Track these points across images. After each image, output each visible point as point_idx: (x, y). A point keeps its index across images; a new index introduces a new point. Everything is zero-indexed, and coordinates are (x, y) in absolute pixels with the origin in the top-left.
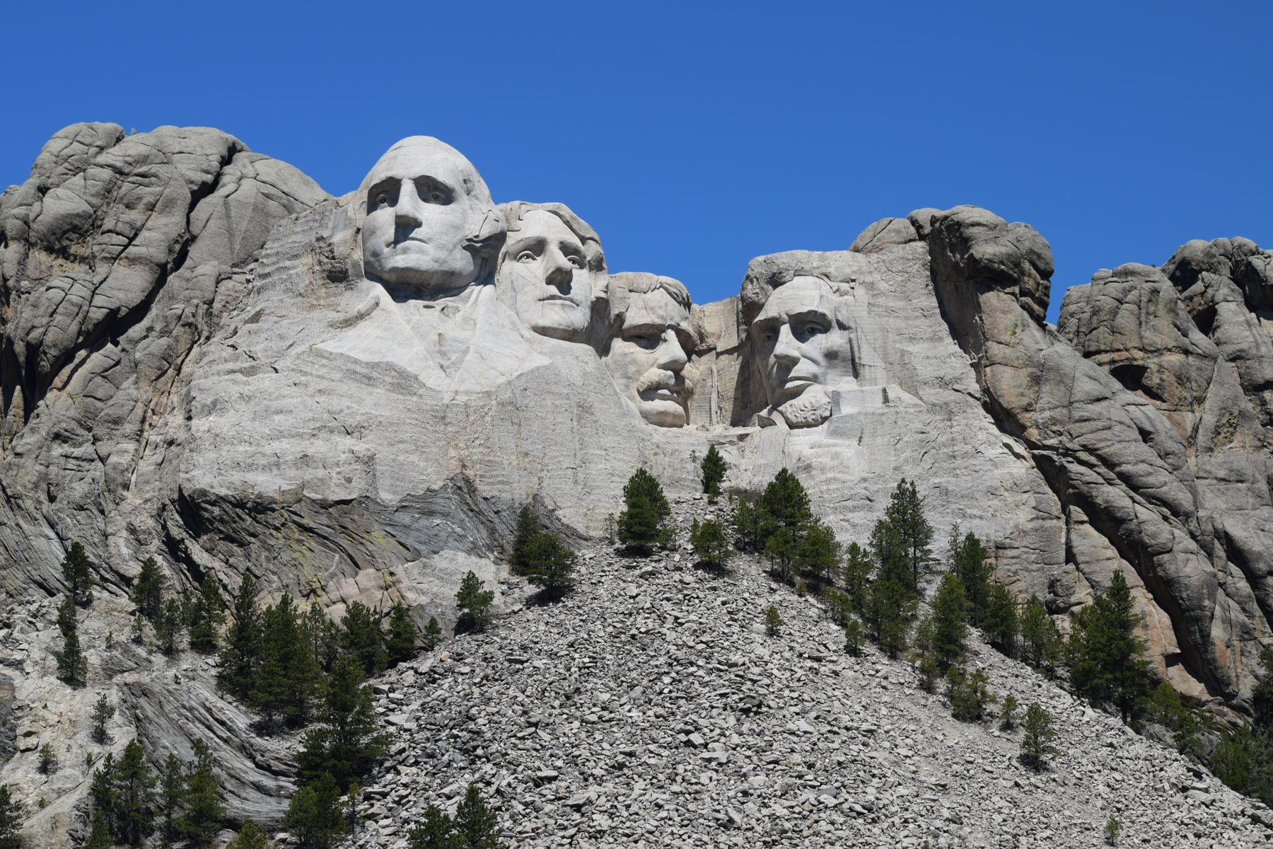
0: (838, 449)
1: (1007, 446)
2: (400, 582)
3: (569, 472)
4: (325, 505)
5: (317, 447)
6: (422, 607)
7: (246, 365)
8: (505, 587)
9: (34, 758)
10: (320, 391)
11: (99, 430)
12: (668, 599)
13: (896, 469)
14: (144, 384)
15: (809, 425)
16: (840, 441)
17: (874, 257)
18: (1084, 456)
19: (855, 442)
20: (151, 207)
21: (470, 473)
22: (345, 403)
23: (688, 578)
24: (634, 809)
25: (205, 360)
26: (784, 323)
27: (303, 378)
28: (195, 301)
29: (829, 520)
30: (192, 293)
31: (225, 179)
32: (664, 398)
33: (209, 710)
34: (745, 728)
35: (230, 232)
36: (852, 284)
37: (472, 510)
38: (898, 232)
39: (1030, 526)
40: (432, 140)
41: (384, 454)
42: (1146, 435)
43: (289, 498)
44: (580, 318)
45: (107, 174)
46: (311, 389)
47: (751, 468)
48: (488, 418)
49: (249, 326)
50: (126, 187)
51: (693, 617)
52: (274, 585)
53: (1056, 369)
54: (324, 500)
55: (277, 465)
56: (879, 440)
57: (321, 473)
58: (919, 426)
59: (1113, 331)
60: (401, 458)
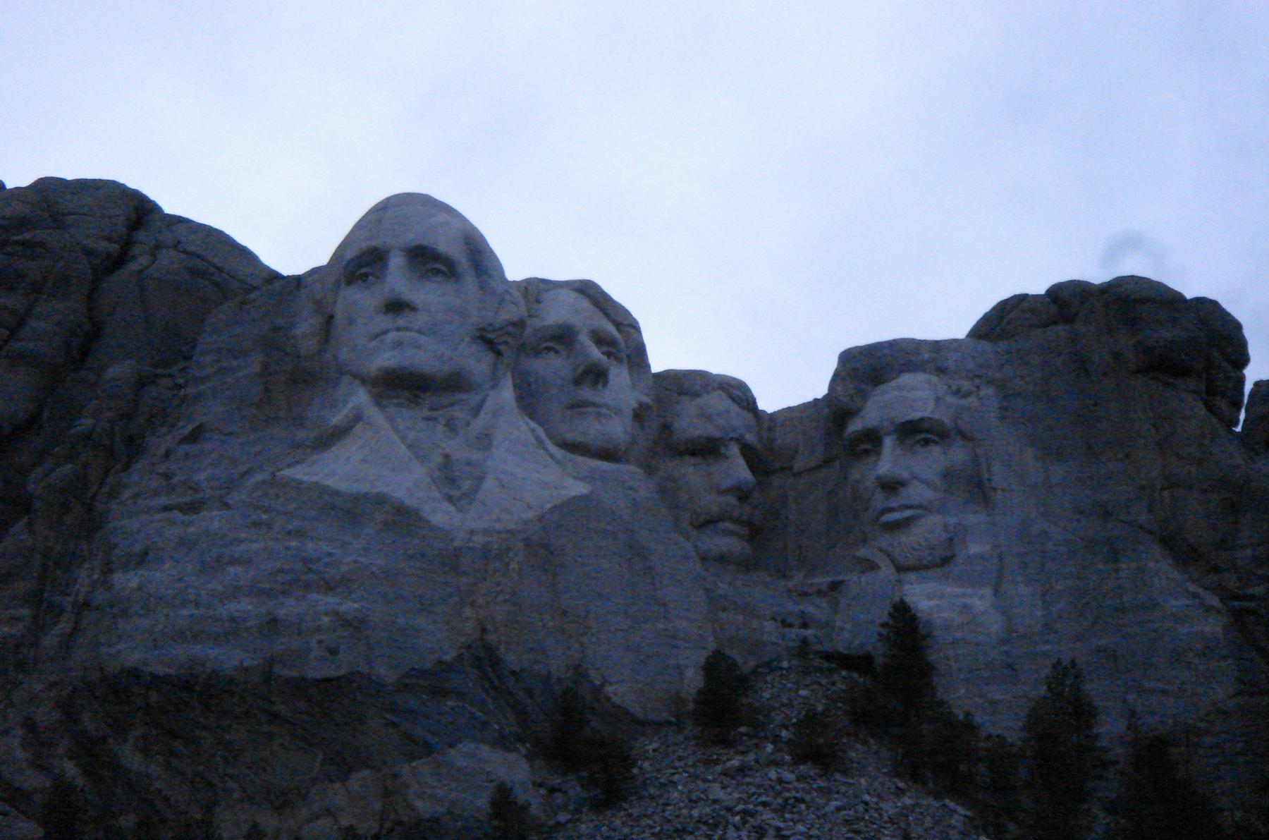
0: (968, 601)
1: (1195, 595)
2: (407, 786)
3: (619, 634)
4: (300, 686)
5: (289, 608)
6: (435, 820)
7: (188, 499)
8: (543, 791)
10: (289, 533)
12: (765, 804)
13: (1045, 625)
15: (926, 568)
16: (969, 590)
17: (1003, 345)
19: (988, 591)
20: (37, 288)
21: (491, 638)
22: (325, 547)
23: (788, 776)
25: (126, 495)
26: (888, 434)
27: (265, 517)
28: (109, 414)
29: (959, 696)
31: (137, 250)
36: (977, 381)
37: (495, 688)
44: (618, 429)
47: (857, 626)
48: (514, 565)
49: (185, 447)
51: (800, 827)
52: (235, 796)
54: (303, 679)
60: (401, 621)
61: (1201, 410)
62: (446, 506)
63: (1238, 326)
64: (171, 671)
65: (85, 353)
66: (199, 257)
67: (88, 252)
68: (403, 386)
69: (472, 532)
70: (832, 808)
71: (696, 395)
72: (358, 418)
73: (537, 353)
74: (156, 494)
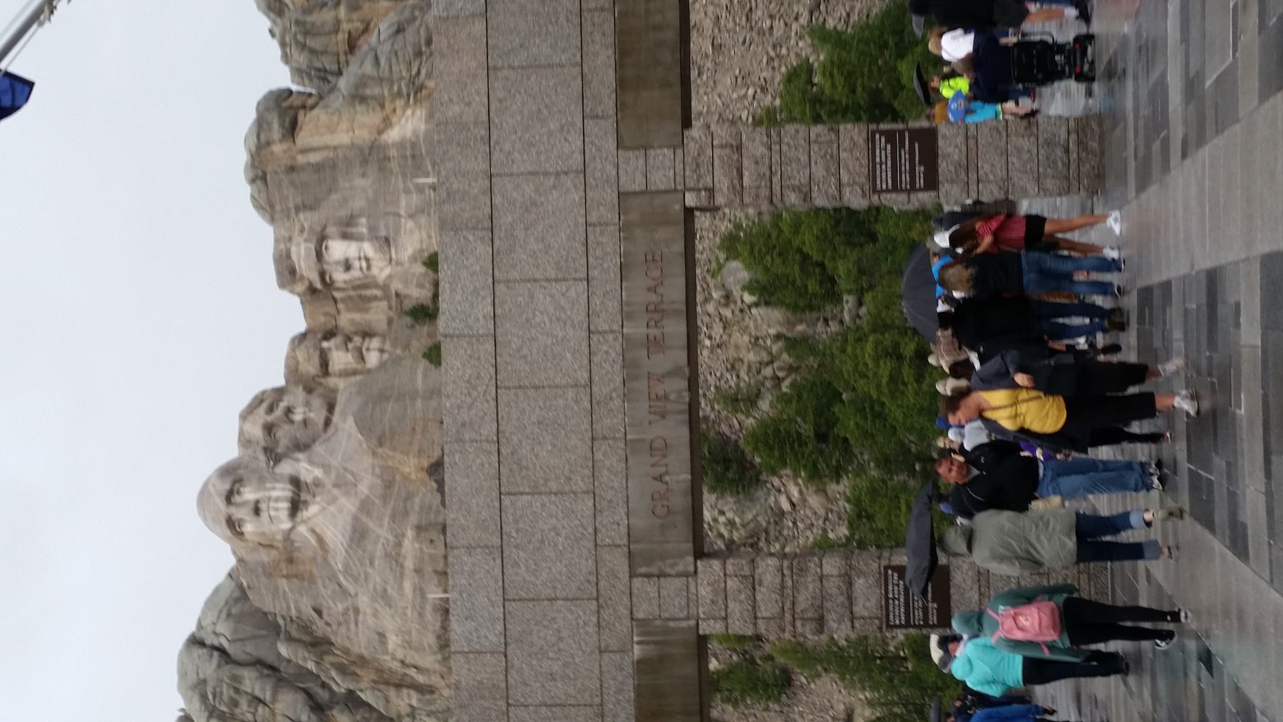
5: (409, 564)
7: (351, 614)
14: (363, 685)
18: (414, 71)
20: (237, 691)
25: (347, 644)
30: (300, 655)
31: (216, 643)
35: (254, 637)
41: (414, 519)
42: (400, 30)
46: (370, 571)
53: (357, 87)
55: (421, 589)
57: (426, 557)
59: (324, 52)
60: (417, 508)
61: (315, 112)
62: (360, 487)
63: (271, 93)
64: (439, 618)
65: (272, 668)
66: (221, 611)
67: (219, 666)
68: (296, 506)
69: (373, 474)
71: (298, 363)
72: (313, 531)
73: (277, 442)
74: (349, 629)
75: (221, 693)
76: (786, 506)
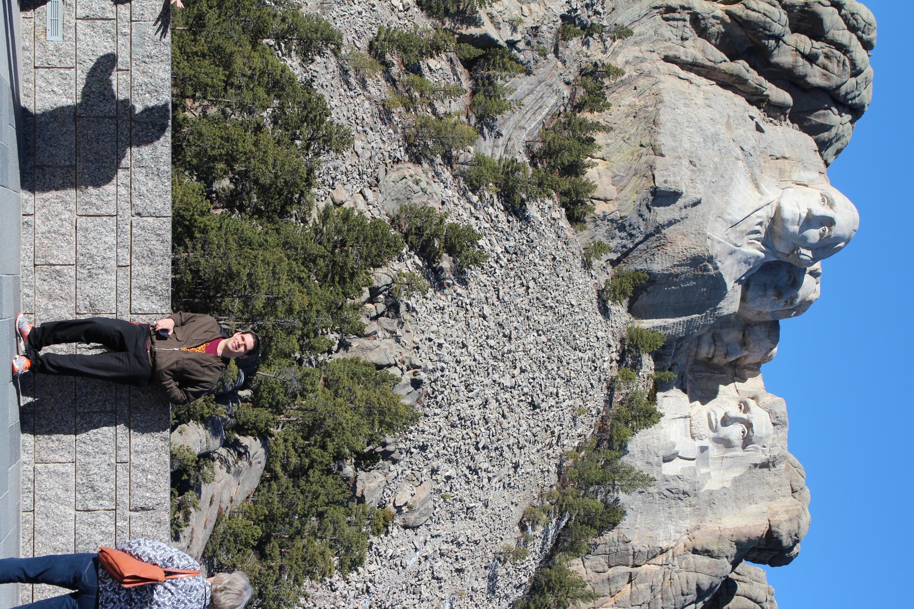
4: (651, 167)
9: (516, 13)
11: (701, 42)
13: (664, 476)
24: (480, 341)
32: (710, 348)
33: (540, 107)
34: (523, 398)
36: (768, 455)
38: (797, 481)
39: (630, 548)
40: (856, 227)
43: (657, 147)
45: (845, 41)
50: (838, 53)
56: (680, 467)
58: (687, 488)
63: (787, 564)
70: (592, 381)
75: (838, 66)
76: (368, 192)
